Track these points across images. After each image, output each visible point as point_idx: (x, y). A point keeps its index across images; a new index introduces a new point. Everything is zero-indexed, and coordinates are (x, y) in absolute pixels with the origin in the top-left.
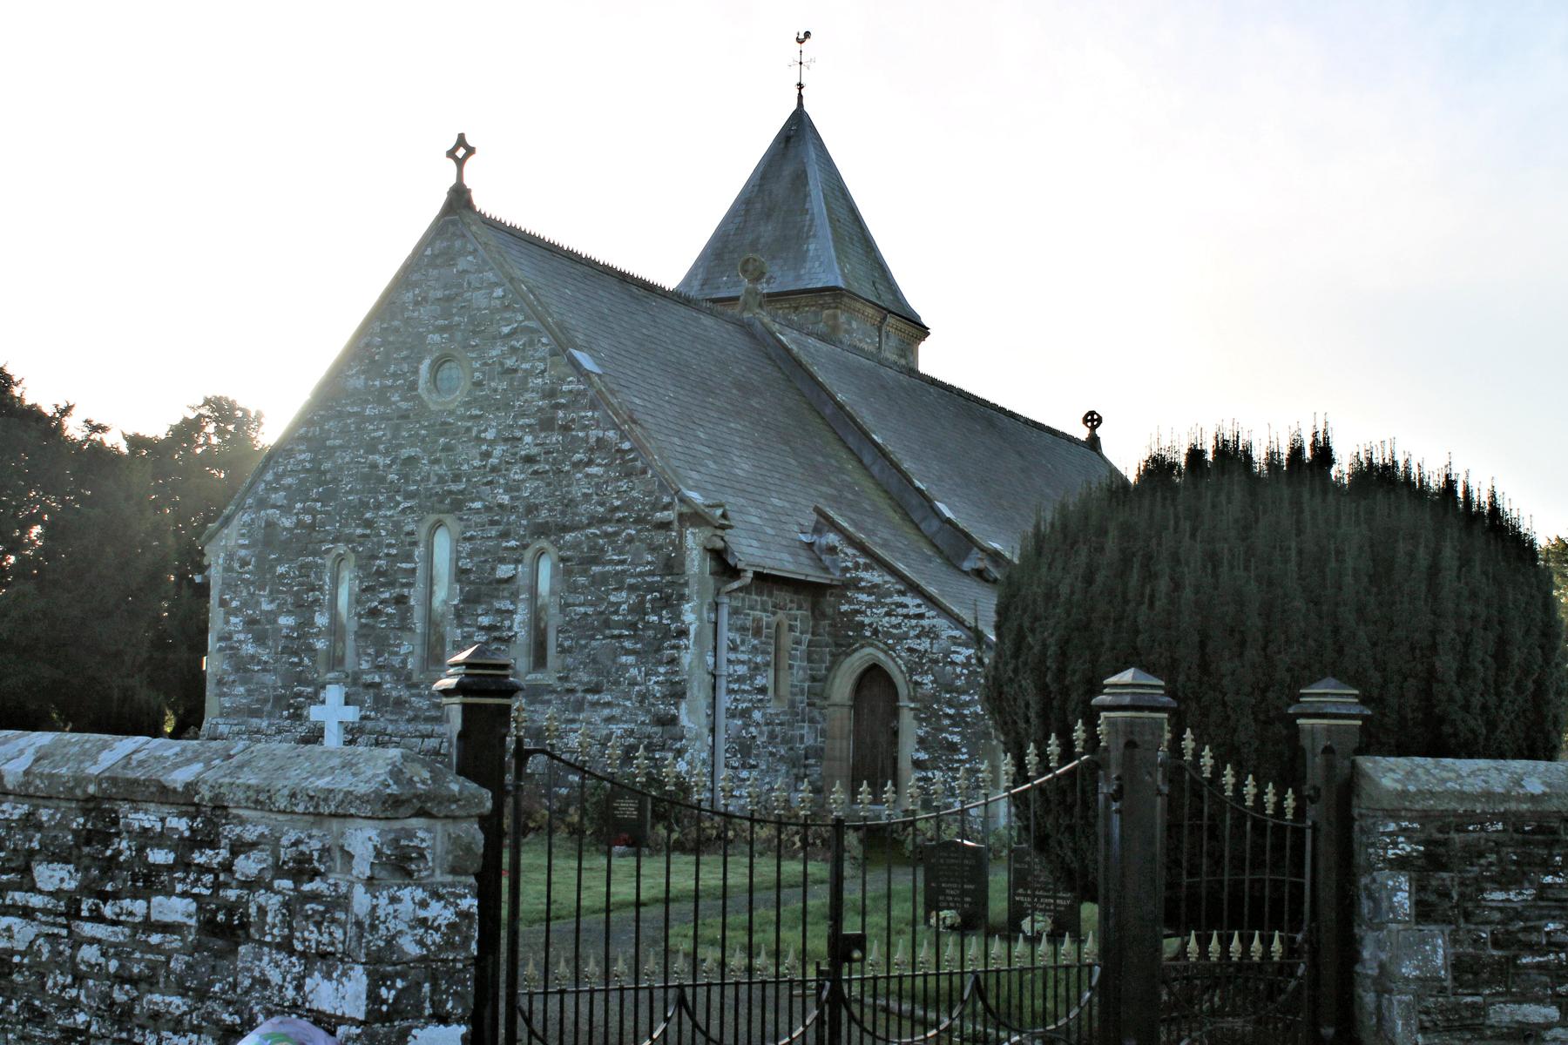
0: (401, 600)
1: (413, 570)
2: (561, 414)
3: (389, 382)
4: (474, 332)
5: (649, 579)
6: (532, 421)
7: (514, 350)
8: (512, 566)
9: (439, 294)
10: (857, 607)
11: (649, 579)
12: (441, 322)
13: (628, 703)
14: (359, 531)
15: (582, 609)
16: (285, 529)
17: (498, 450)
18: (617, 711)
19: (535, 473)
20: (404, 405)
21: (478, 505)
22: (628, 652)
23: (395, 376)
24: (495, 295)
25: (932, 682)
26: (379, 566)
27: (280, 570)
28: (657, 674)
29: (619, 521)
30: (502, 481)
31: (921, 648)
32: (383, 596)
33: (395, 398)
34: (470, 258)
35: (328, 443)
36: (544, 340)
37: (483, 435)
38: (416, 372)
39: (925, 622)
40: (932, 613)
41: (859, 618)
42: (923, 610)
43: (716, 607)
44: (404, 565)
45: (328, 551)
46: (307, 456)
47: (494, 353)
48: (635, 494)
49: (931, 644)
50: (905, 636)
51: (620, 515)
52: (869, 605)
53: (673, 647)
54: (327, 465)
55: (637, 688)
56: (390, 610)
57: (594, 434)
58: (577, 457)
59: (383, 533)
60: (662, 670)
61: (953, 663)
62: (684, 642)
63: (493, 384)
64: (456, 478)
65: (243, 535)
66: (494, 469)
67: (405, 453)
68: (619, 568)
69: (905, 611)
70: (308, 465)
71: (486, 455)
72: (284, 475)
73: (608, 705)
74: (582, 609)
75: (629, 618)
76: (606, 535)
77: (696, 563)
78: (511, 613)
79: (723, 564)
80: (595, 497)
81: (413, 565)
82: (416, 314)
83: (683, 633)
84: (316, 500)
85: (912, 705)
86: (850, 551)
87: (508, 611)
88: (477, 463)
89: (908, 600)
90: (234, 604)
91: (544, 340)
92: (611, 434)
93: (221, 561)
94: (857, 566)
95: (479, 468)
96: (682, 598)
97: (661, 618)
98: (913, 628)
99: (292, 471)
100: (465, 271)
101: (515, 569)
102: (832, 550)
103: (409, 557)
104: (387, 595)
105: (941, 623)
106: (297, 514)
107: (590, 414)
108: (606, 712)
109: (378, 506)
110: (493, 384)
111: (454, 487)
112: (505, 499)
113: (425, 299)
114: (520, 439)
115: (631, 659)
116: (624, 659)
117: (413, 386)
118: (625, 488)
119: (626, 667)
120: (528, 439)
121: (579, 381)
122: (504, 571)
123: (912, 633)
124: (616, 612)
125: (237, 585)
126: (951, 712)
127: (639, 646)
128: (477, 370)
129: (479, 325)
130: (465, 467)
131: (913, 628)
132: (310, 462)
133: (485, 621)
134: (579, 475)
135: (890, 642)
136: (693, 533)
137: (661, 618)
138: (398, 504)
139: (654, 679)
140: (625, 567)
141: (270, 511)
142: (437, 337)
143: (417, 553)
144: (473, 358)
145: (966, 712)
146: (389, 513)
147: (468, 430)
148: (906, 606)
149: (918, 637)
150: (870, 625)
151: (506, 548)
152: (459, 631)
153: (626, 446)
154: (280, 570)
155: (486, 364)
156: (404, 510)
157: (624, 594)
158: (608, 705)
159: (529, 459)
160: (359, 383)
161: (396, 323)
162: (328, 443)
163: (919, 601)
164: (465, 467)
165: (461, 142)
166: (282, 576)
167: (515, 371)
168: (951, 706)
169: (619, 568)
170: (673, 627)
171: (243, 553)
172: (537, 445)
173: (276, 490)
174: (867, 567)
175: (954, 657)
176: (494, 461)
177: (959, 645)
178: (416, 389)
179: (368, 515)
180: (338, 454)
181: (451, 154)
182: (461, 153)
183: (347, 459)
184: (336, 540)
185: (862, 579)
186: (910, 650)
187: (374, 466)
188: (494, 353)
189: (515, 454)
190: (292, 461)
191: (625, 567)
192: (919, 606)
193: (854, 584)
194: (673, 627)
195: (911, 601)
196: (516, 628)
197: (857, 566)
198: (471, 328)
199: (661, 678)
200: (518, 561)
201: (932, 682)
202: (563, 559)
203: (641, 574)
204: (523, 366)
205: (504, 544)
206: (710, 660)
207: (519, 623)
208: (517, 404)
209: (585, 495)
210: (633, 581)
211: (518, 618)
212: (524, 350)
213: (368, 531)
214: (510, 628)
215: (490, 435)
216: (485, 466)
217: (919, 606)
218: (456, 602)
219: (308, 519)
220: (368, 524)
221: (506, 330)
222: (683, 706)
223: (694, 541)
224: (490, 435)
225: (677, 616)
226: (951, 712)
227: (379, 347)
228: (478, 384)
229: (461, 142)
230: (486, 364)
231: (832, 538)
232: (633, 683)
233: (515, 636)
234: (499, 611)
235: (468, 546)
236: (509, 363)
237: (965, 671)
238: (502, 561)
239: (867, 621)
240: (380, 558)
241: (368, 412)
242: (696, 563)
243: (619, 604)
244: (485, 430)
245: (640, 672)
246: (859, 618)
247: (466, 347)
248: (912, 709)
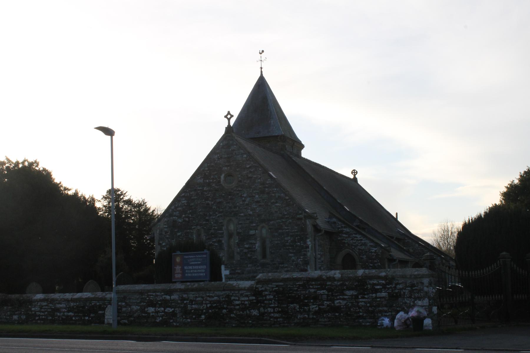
0: (220, 242)
1: (223, 233)
2: (267, 189)
3: (211, 181)
5: (296, 233)
6: (258, 191)
7: (251, 172)
8: (254, 231)
9: (226, 156)
10: (343, 238)
11: (296, 233)
12: (227, 164)
13: (292, 267)
14: (204, 222)
15: (277, 242)
16: (179, 222)
17: (248, 199)
18: (289, 269)
19: (260, 205)
20: (216, 187)
21: (242, 214)
22: (291, 253)
23: (213, 179)
24: (244, 157)
25: (366, 258)
26: (212, 232)
27: (179, 234)
28: (301, 258)
29: (286, 218)
30: (250, 208)
31: (362, 248)
32: (213, 240)
33: (214, 185)
34: (235, 146)
35: (192, 198)
36: (260, 169)
37: (243, 195)
38: (220, 178)
39: (363, 241)
40: (365, 239)
41: (344, 241)
42: (362, 238)
43: (315, 240)
44: (220, 232)
45: (194, 228)
46: (186, 202)
47: (245, 173)
48: (291, 211)
49: (365, 247)
50: (357, 245)
51: (286, 216)
52: (346, 237)
53: (304, 251)
54: (192, 204)
55: (295, 262)
56: (216, 244)
57: (277, 195)
58: (272, 201)
59: (212, 223)
60: (302, 257)
61: (372, 252)
62: (307, 250)
63: (245, 181)
64: (235, 207)
65: (165, 225)
66: (247, 205)
67: (218, 200)
68: (287, 231)
69: (357, 239)
70: (186, 204)
71: (244, 201)
72: (178, 207)
73: (286, 267)
74: (277, 242)
75: (291, 244)
76: (283, 222)
77: (310, 229)
78: (255, 244)
79: (317, 229)
80: (278, 212)
81: (223, 232)
82: (219, 162)
83: (308, 247)
84: (189, 214)
85: (361, 264)
86: (340, 223)
87: (254, 243)
88: (241, 203)
89: (357, 236)
90: (164, 244)
91: (260, 169)
92: (282, 195)
93: (158, 232)
94: (342, 227)
95: (242, 204)
96: (307, 238)
97: (300, 243)
98: (359, 243)
99: (180, 206)
100: (234, 150)
101: (256, 232)
102: (335, 223)
103: (221, 229)
104: (215, 240)
105: (367, 241)
106: (183, 218)
107: (275, 189)
108: (286, 269)
109: (210, 215)
110: (245, 181)
111: (235, 210)
112: (251, 213)
113: (221, 158)
114: (254, 196)
115: (292, 255)
116: (290, 255)
117: (219, 182)
118: (288, 209)
119: (291, 257)
120: (257, 196)
121: (272, 180)
122: (252, 232)
123: (359, 245)
124: (287, 242)
125: (164, 239)
126: (371, 265)
127: (294, 251)
130: (238, 204)
131: (359, 243)
132: (186, 203)
133: (247, 246)
134: (273, 206)
135: (353, 247)
136: (308, 221)
137: (300, 243)
138: (216, 215)
139: (299, 260)
140: (289, 230)
141: (174, 218)
142: (226, 168)
143: (224, 228)
145: (376, 265)
146: (214, 217)
147: (238, 194)
148: (357, 237)
149: (361, 245)
150: (347, 243)
151: (252, 226)
152: (239, 249)
153: (287, 198)
154: (179, 234)
156: (218, 217)
157: (289, 238)
158: (286, 267)
159: (258, 202)
160: (201, 181)
161: (212, 164)
162: (192, 198)
163: (360, 236)
164: (238, 204)
165: (229, 113)
166: (179, 236)
167: (251, 178)
168: (371, 264)
169: (287, 231)
170: (304, 246)
171: (166, 229)
172: (260, 198)
173: (175, 212)
174: (345, 227)
175: (372, 250)
176: (247, 202)
177: (373, 247)
178: (220, 183)
179: (207, 218)
180: (196, 201)
181: (226, 117)
182: (229, 116)
183: (199, 202)
184: (197, 225)
185: (344, 231)
186: (359, 249)
187: (208, 204)
188: (245, 173)
189: (253, 200)
190: (180, 203)
191: (289, 230)
192: (361, 237)
193: (342, 232)
194: (304, 246)
195: (358, 236)
196: (257, 248)
197: (342, 227)
199: (302, 259)
200: (256, 230)
201: (366, 258)
202: (270, 229)
203: (294, 232)
204: (254, 176)
205: (251, 225)
206: (314, 254)
207: (258, 245)
208: (253, 187)
209: (275, 211)
210: (291, 234)
211: (257, 245)
213: (207, 222)
214: (255, 248)
215: (245, 195)
216: (244, 204)
217: (361, 237)
218: (237, 241)
219: (187, 219)
220: (207, 220)
221: (248, 166)
222: (309, 267)
223: (309, 222)
224: (245, 195)
225: (305, 243)
226: (371, 265)
227: (207, 171)
228: (240, 181)
229: (229, 113)
231: (334, 220)
232: (293, 261)
233: (257, 249)
234: (251, 243)
235: (240, 226)
236: (250, 175)
237: (375, 254)
238: (251, 230)
239: (346, 242)
240: (212, 230)
241: (205, 189)
242: (310, 229)
243: (288, 240)
244: (243, 194)
245: (295, 258)
246: (344, 241)
248: (361, 265)
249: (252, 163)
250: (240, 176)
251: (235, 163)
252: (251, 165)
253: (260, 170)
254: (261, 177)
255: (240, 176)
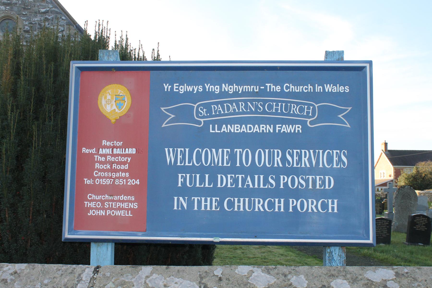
4: (24, 9)
7: (46, 20)
36: (63, 18)
47: (36, 19)
91: (63, 18)
128: (26, 25)
129: (27, 6)
144: (24, 20)
155: (31, 23)
188: (36, 19)
198: (23, 6)
212: (52, 20)
221: (43, 10)
230: (31, 23)
247: (20, 14)
249: (51, 6)
250: (27, 23)
251: (20, 2)
252: (48, 9)
253: (63, 19)
254: (64, 31)
255: (27, 23)
